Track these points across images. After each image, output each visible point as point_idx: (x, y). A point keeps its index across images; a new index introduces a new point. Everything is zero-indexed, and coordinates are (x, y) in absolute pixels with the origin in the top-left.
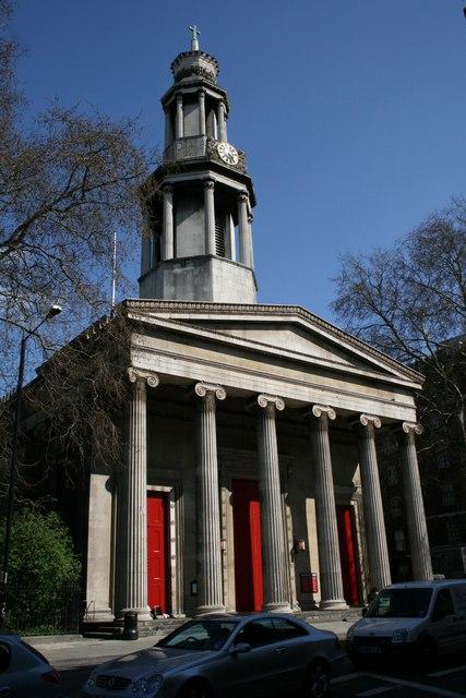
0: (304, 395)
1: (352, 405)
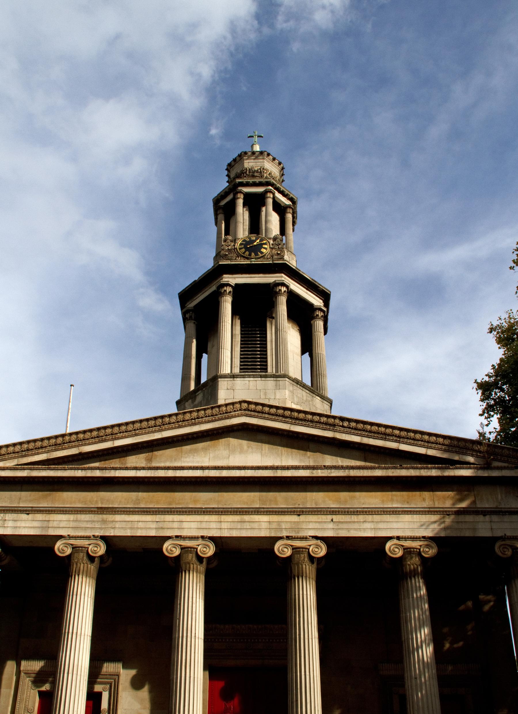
0: (259, 527)
1: (365, 528)
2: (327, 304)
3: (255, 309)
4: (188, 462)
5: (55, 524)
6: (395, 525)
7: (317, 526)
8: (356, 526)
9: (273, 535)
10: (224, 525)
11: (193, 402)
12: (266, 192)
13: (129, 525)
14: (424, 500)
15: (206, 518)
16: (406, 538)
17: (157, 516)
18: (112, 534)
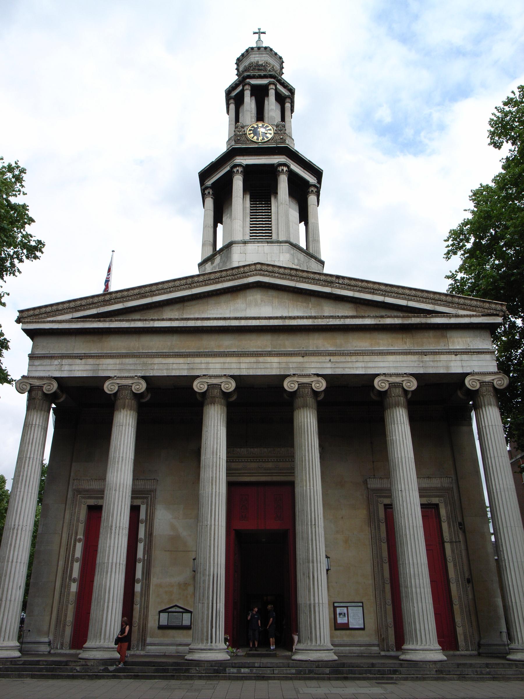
0: (271, 366)
1: (357, 367)
2: (319, 181)
3: (261, 186)
4: (213, 314)
5: (104, 367)
6: (382, 364)
7: (318, 365)
8: (350, 365)
9: (282, 373)
10: (243, 366)
11: (212, 263)
12: (270, 84)
13: (166, 367)
14: (406, 343)
15: (228, 360)
16: (391, 375)
17: (188, 359)
18: (151, 375)
